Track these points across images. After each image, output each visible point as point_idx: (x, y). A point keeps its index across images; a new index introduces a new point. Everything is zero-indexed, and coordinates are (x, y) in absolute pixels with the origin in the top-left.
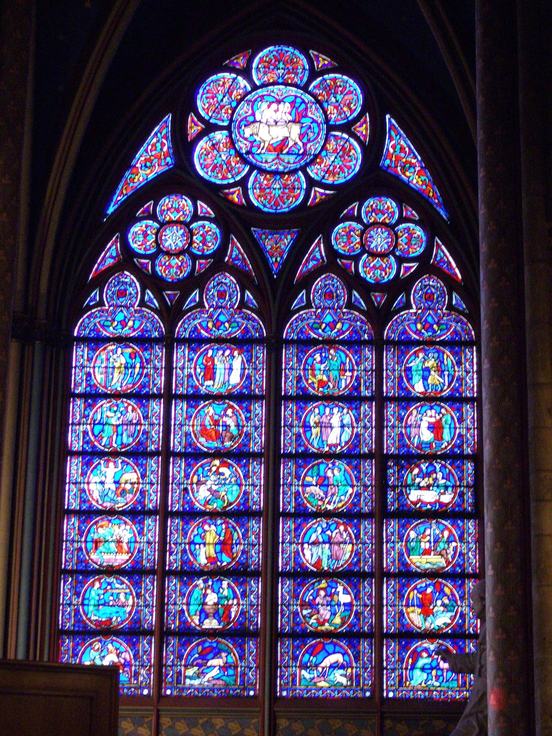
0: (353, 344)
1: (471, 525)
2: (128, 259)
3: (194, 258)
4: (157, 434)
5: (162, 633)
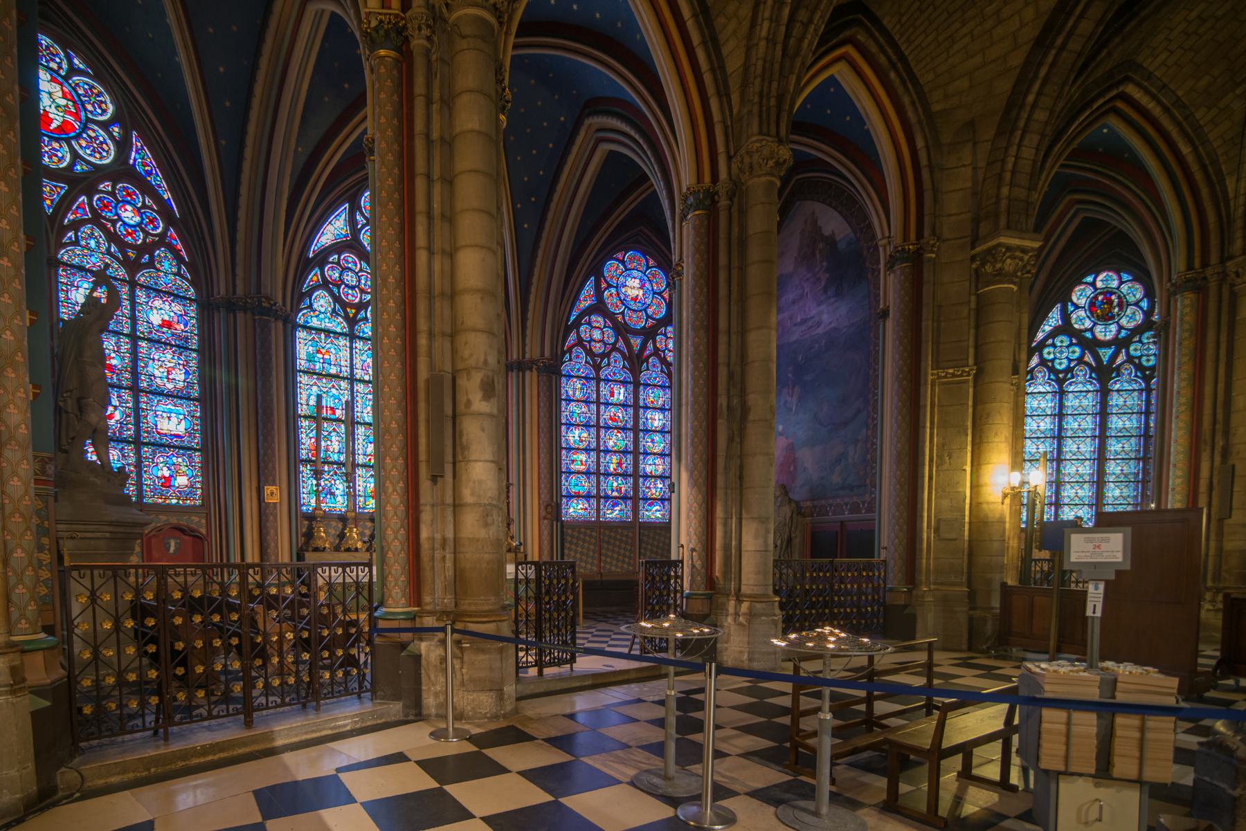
0: (663, 387)
1: (667, 459)
2: (580, 342)
3: (605, 344)
4: (594, 418)
5: (598, 497)
